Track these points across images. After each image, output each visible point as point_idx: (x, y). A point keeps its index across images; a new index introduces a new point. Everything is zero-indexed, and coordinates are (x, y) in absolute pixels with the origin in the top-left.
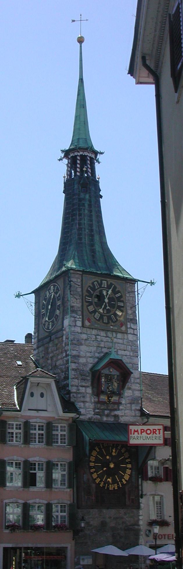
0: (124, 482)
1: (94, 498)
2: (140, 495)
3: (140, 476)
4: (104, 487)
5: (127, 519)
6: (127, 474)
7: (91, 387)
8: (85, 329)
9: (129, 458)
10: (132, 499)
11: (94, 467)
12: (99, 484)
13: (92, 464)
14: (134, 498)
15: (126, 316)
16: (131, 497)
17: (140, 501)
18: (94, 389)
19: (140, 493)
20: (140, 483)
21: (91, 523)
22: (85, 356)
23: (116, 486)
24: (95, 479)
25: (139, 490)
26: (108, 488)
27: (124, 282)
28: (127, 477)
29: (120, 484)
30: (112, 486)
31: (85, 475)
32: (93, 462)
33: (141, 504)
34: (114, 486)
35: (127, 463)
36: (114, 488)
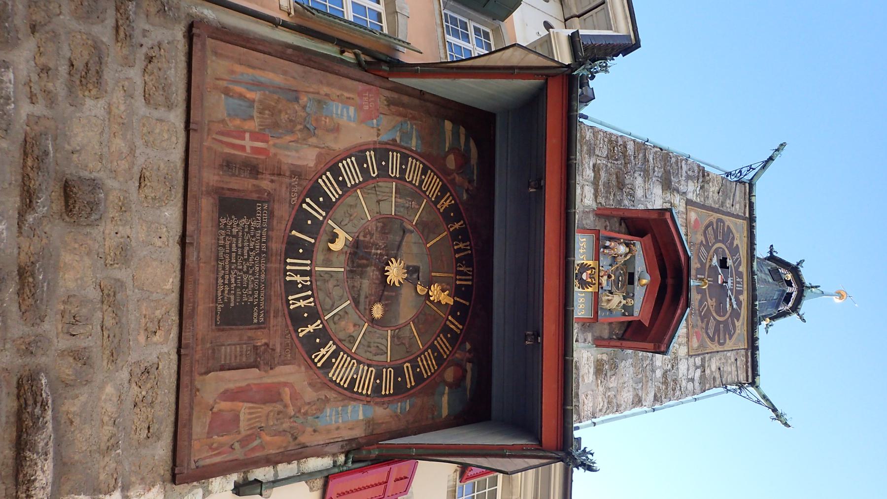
0: (323, 351)
1: (248, 150)
2: (251, 477)
3: (341, 459)
4: (300, 220)
5: (109, 389)
6: (357, 372)
7: (595, 206)
8: (684, 210)
9: (419, 378)
10: (236, 419)
11: (383, 172)
12: (315, 192)
13: (395, 159)
14: (243, 425)
15: (707, 353)
16: (244, 409)
17: (217, 483)
18: (592, 217)
19: (262, 474)
20: (314, 464)
21: (89, 102)
22: (646, 196)
23: (302, 303)
24: (336, 172)
25: (272, 461)
26: (293, 248)
27: (746, 347)
28: (341, 373)
29: (311, 328)
30: (303, 273)
31: (352, 110)
32: (403, 172)
33: (199, 492)
34: (305, 288)
35: (399, 372)
36: (292, 287)
